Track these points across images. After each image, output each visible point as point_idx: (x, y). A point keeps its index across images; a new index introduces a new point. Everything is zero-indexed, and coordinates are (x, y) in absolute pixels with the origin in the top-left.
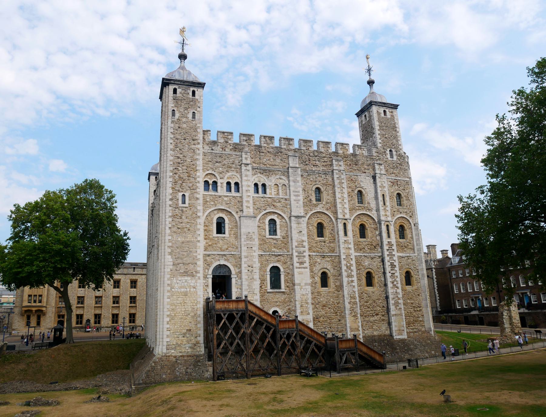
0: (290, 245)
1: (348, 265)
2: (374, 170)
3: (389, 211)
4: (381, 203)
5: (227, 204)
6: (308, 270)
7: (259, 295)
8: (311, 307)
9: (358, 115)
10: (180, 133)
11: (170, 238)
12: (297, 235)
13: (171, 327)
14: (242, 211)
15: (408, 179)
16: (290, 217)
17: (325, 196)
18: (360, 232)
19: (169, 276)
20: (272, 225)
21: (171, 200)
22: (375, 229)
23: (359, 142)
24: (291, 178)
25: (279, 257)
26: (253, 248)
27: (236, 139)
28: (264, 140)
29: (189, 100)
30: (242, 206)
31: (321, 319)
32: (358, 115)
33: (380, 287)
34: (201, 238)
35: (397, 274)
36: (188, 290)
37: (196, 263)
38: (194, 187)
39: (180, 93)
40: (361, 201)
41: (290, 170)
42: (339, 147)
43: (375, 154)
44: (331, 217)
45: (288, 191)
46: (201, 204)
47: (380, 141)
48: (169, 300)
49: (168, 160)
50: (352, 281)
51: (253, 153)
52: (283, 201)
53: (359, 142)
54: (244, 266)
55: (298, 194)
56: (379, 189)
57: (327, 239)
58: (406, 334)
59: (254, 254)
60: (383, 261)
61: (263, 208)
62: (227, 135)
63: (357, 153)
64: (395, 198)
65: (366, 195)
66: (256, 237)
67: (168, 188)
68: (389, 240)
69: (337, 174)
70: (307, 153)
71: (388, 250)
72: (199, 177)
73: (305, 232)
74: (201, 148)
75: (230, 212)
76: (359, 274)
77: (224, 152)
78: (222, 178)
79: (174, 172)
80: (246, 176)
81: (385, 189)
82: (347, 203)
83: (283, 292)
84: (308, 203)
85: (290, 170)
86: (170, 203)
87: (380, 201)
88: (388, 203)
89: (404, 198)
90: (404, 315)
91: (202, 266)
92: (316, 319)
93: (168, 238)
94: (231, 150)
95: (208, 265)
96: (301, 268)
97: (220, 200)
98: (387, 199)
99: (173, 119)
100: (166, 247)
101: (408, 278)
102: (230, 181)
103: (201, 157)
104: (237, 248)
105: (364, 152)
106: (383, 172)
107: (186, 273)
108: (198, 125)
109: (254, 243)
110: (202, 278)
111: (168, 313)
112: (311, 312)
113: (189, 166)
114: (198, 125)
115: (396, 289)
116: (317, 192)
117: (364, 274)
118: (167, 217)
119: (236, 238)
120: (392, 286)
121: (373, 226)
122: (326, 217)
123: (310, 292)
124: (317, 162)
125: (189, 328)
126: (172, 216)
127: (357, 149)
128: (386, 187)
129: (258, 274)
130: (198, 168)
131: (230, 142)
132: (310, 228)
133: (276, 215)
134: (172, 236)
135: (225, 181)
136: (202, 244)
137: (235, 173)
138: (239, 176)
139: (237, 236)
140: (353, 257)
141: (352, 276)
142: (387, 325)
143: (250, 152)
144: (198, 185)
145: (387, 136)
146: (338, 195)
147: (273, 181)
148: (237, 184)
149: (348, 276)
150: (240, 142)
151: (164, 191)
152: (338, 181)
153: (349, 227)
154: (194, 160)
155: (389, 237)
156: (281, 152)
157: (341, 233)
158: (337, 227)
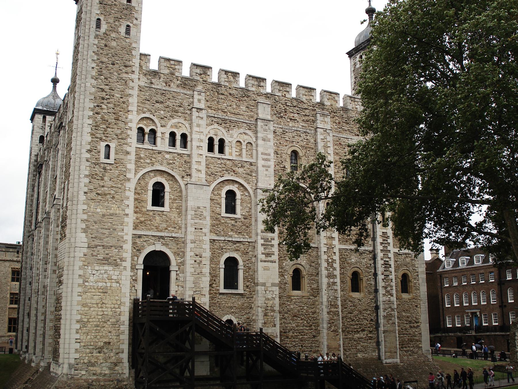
1: (330, 261)
5: (169, 164)
6: (276, 265)
7: (208, 296)
8: (278, 316)
9: (350, 54)
10: (107, 55)
11: (85, 207)
13: (82, 338)
19: (81, 264)
21: (89, 151)
24: (260, 135)
25: (238, 245)
26: (204, 230)
27: (186, 72)
28: (225, 76)
30: (190, 168)
31: (291, 334)
32: (350, 54)
33: (370, 293)
34: (130, 211)
35: (392, 277)
36: (109, 284)
37: (122, 247)
38: (124, 136)
41: (258, 123)
45: (254, 152)
46: (133, 162)
48: (80, 298)
51: (208, 93)
52: (247, 166)
54: (189, 254)
58: (398, 357)
60: (374, 258)
61: (219, 174)
62: (171, 64)
63: (350, 107)
66: (207, 214)
67: (85, 133)
68: (385, 231)
69: (321, 134)
71: (382, 243)
72: (131, 121)
74: (137, 80)
75: (173, 176)
77: (167, 88)
78: (164, 126)
79: (95, 111)
80: (198, 126)
85: (260, 123)
86: (88, 155)
90: (397, 332)
91: (130, 251)
92: (283, 333)
95: (138, 250)
99: (98, 33)
100: (79, 221)
101: (405, 283)
103: (135, 92)
104: (180, 228)
107: (106, 261)
108: (134, 45)
109: (204, 222)
110: (129, 269)
111: (79, 317)
112: (278, 323)
114: (134, 45)
115: (388, 297)
116: (293, 158)
117: (349, 274)
118: (82, 176)
119: (180, 213)
124: (296, 115)
125: (107, 340)
129: (208, 267)
130: (130, 108)
131: (177, 74)
133: (237, 186)
134: (88, 205)
136: (130, 220)
137: (182, 120)
138: (187, 125)
139: (180, 211)
140: (336, 250)
141: (334, 276)
142: (374, 344)
144: (129, 132)
148: (184, 136)
149: (329, 276)
150: (191, 75)
151: (79, 138)
154: (124, 95)
156: (248, 97)
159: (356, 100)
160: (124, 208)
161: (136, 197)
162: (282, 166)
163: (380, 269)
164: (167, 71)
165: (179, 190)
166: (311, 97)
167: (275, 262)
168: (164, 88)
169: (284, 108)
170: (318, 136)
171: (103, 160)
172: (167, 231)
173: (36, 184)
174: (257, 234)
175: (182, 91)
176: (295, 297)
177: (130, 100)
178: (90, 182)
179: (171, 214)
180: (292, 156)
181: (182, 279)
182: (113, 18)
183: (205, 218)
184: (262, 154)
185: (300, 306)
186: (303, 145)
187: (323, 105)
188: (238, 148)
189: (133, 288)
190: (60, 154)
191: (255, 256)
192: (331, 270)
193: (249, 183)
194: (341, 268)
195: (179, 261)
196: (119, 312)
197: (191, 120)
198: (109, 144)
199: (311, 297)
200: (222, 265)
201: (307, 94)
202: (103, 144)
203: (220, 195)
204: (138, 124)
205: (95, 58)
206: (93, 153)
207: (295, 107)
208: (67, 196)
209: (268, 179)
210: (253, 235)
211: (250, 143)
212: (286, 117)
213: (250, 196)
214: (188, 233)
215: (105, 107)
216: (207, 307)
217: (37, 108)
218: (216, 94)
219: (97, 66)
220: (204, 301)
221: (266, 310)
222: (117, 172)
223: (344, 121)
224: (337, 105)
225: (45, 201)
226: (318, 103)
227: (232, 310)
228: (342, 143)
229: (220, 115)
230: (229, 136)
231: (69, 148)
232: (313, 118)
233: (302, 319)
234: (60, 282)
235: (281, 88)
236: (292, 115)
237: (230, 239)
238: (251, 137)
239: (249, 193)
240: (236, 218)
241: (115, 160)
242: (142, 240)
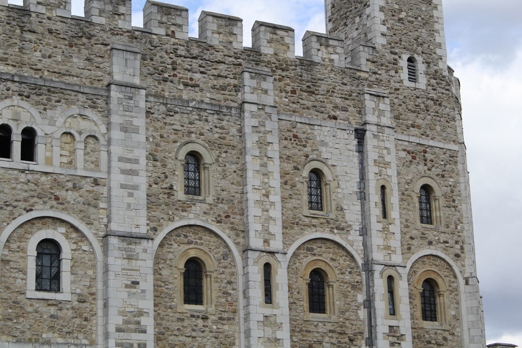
0: (100, 321)
2: (361, 112)
3: (398, 236)
4: (375, 212)
12: (124, 294)
15: (455, 147)
16: (106, 236)
17: (212, 179)
18: (311, 295)
20: (46, 260)
22: (354, 287)
23: (320, 27)
24: (115, 119)
40: (317, 203)
42: (265, 35)
43: (366, 66)
44: (230, 242)
45: (104, 155)
47: (384, 29)
52: (87, 186)
53: (320, 27)
55: (134, 167)
56: (372, 170)
57: (212, 309)
63: (316, 59)
64: (416, 200)
65: (333, 185)
68: (393, 323)
69: (253, 116)
73: (147, 284)
81: (389, 172)
82: (279, 206)
84: (159, 200)
85: (115, 93)
87: (372, 205)
88: (394, 213)
89: (442, 202)
98: (394, 199)
105: (334, 57)
106: (386, 120)
116: (192, 167)
121: (348, 277)
122: (214, 239)
124: (198, 76)
127: (315, 45)
128: (394, 166)
132: (165, 272)
133: (63, 230)
145: (403, 15)
146: (253, 179)
147: (60, 121)
152: (255, 137)
153: (281, 277)
155: (393, 312)
157: (257, 292)
158: (246, 274)
159: (331, 42)
169: (170, 61)
170: (246, 120)
174: (107, 336)
180: (188, 163)
184: (121, 159)
188: (67, 146)
201: (221, 30)
203: (24, 250)
207: (195, 58)
209: (133, 213)
211: (94, 137)
213: (93, 253)
218: (18, 31)
223: (304, 87)
224: (289, 55)
226: (246, 49)
228: (300, 135)
230: (47, 122)
232: (236, 82)
238: (96, 124)
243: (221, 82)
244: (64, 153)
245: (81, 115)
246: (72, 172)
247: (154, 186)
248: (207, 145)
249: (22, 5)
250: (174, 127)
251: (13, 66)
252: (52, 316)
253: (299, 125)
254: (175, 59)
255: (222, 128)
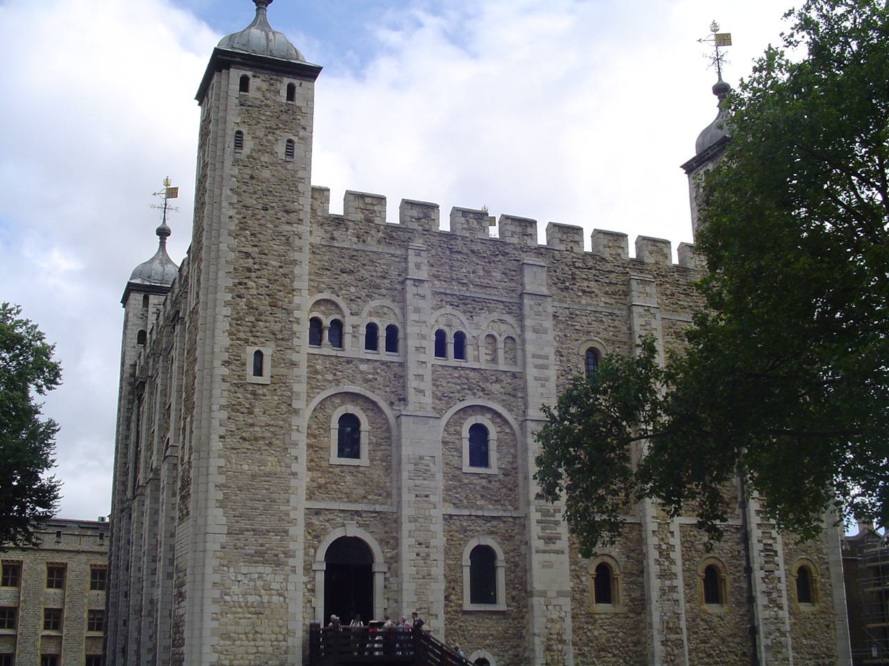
1: (664, 547)
5: (367, 381)
6: (565, 558)
7: (442, 616)
9: (689, 168)
11: (222, 462)
14: (404, 400)
19: (216, 562)
21: (226, 363)
23: (690, 240)
24: (528, 322)
25: (494, 523)
26: (432, 498)
29: (278, 109)
30: (404, 387)
32: (689, 168)
33: (739, 604)
34: (301, 466)
35: (781, 573)
36: (265, 599)
37: (286, 532)
38: (286, 334)
39: (259, 89)
48: (215, 624)
49: (222, 261)
50: (673, 589)
51: (433, 252)
54: (407, 542)
59: (433, 512)
60: (746, 539)
61: (457, 395)
62: (366, 204)
66: (438, 470)
67: (217, 332)
69: (641, 316)
70: (569, 260)
75: (374, 403)
76: (688, 570)
77: (360, 246)
78: (357, 314)
83: (502, 613)
85: (527, 301)
86: (226, 371)
91: (301, 539)
93: (215, 462)
94: (379, 242)
96: (549, 552)
97: (349, 370)
100: (211, 487)
101: (805, 586)
102: (375, 320)
103: (305, 257)
104: (389, 495)
107: (261, 557)
108: (301, 174)
109: (433, 484)
110: (300, 570)
113: (271, 277)
114: (301, 174)
116: (591, 361)
117: (701, 570)
118: (215, 407)
119: (388, 469)
120: (766, 603)
123: (569, 615)
124: (593, 284)
126: (227, 406)
129: (441, 564)
130: (296, 285)
133: (489, 416)
135: (363, 322)
138: (397, 311)
139: (390, 464)
143: (427, 250)
144: (295, 327)
148: (392, 331)
149: (662, 576)
151: (208, 341)
156: (505, 254)
160: (288, 461)
161: (309, 441)
162: (570, 377)
163: (758, 559)
164: (359, 216)
165: (385, 427)
166: (620, 251)
167: (563, 553)
168: (355, 247)
169: (570, 273)
171: (251, 377)
172: (365, 500)
173: (134, 417)
174: (528, 503)
175: (387, 250)
176: (603, 616)
177: (297, 270)
178: (229, 418)
179: (371, 471)
180: (588, 358)
181: (394, 587)
182: (263, 130)
183: (433, 476)
184: (534, 356)
185: (611, 632)
186: (607, 337)
187: (642, 263)
188: (490, 347)
189: (308, 605)
190: (175, 366)
191: (526, 543)
192: (667, 563)
193: (510, 410)
194: (685, 560)
195: (389, 555)
196: (284, 648)
197: (404, 300)
198: (262, 349)
199: (631, 615)
200: (466, 560)
201: (611, 244)
202: (251, 350)
203: (459, 433)
204: (311, 311)
205: (235, 199)
206: (233, 367)
207: (590, 269)
208: (190, 442)
210: (521, 504)
212: (575, 287)
213: (514, 434)
214: (404, 504)
215: (254, 285)
216: (440, 638)
217: (133, 281)
218: (448, 252)
219: (237, 213)
220: (436, 627)
221: (549, 640)
222: (276, 398)
224: (667, 263)
225: (149, 448)
226: (632, 260)
227: (488, 642)
229: (456, 289)
230: (473, 326)
231: (191, 359)
232: (624, 288)
233: (614, 656)
234: (181, 595)
235: (565, 237)
236: (586, 284)
237: (480, 513)
239: (511, 427)
240: (490, 475)
241: (272, 377)
242: (321, 519)
243: (613, 288)
244: (487, 351)
245: (500, 320)
246: (494, 367)
247: (561, 378)
248: (603, 342)
249: (449, 230)
250: (577, 327)
251: (445, 281)
252: (483, 487)
253: (678, 323)
254: (574, 270)
255: (614, 327)
